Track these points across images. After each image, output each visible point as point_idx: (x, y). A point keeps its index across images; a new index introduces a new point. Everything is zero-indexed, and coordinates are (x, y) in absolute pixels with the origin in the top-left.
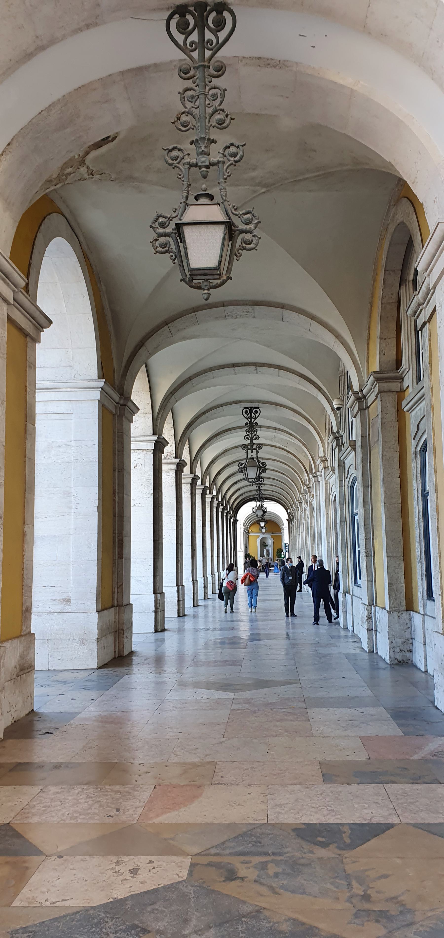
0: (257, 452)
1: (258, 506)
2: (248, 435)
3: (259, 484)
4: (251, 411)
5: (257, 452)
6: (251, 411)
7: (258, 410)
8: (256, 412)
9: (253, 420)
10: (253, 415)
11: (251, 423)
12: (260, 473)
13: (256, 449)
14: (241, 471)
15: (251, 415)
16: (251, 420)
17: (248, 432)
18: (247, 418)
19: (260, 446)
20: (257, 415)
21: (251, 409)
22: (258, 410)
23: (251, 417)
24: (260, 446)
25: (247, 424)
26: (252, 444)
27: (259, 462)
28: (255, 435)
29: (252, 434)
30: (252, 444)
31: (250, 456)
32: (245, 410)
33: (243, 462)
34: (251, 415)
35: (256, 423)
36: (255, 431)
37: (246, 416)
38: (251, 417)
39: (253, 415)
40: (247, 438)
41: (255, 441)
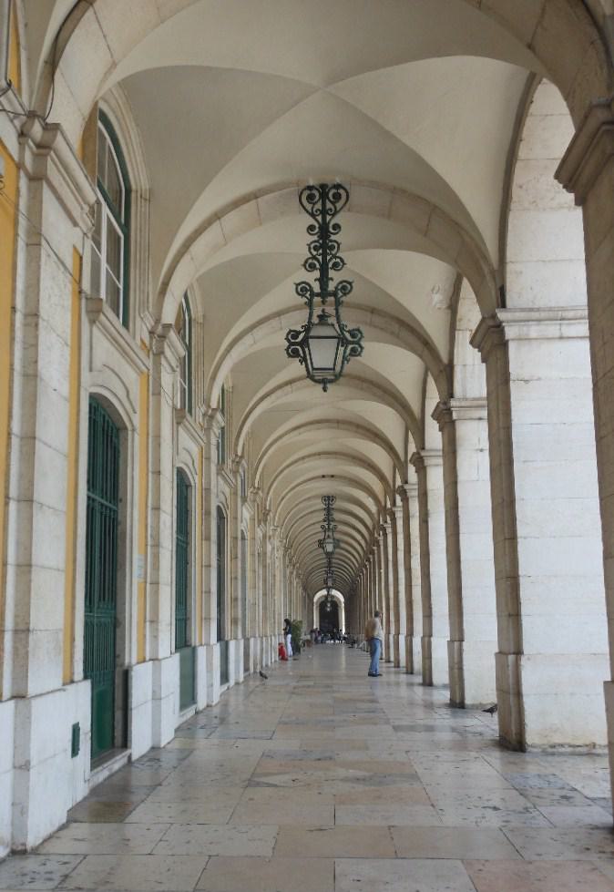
0: (338, 303)
2: (314, 257)
4: (324, 196)
5: (338, 303)
6: (324, 196)
7: (341, 191)
8: (337, 197)
9: (328, 218)
10: (329, 205)
12: (345, 359)
13: (334, 294)
14: (294, 354)
15: (324, 204)
17: (315, 248)
18: (313, 215)
19: (345, 287)
20: (339, 205)
21: (323, 189)
22: (341, 191)
24: (345, 287)
25: (311, 228)
26: (324, 280)
27: (342, 328)
28: (336, 257)
29: (324, 255)
30: (324, 280)
31: (317, 311)
33: (299, 328)
34: (324, 204)
35: (337, 227)
36: (332, 248)
37: (309, 207)
38: (324, 212)
39: (329, 205)
40: (312, 267)
41: (332, 273)
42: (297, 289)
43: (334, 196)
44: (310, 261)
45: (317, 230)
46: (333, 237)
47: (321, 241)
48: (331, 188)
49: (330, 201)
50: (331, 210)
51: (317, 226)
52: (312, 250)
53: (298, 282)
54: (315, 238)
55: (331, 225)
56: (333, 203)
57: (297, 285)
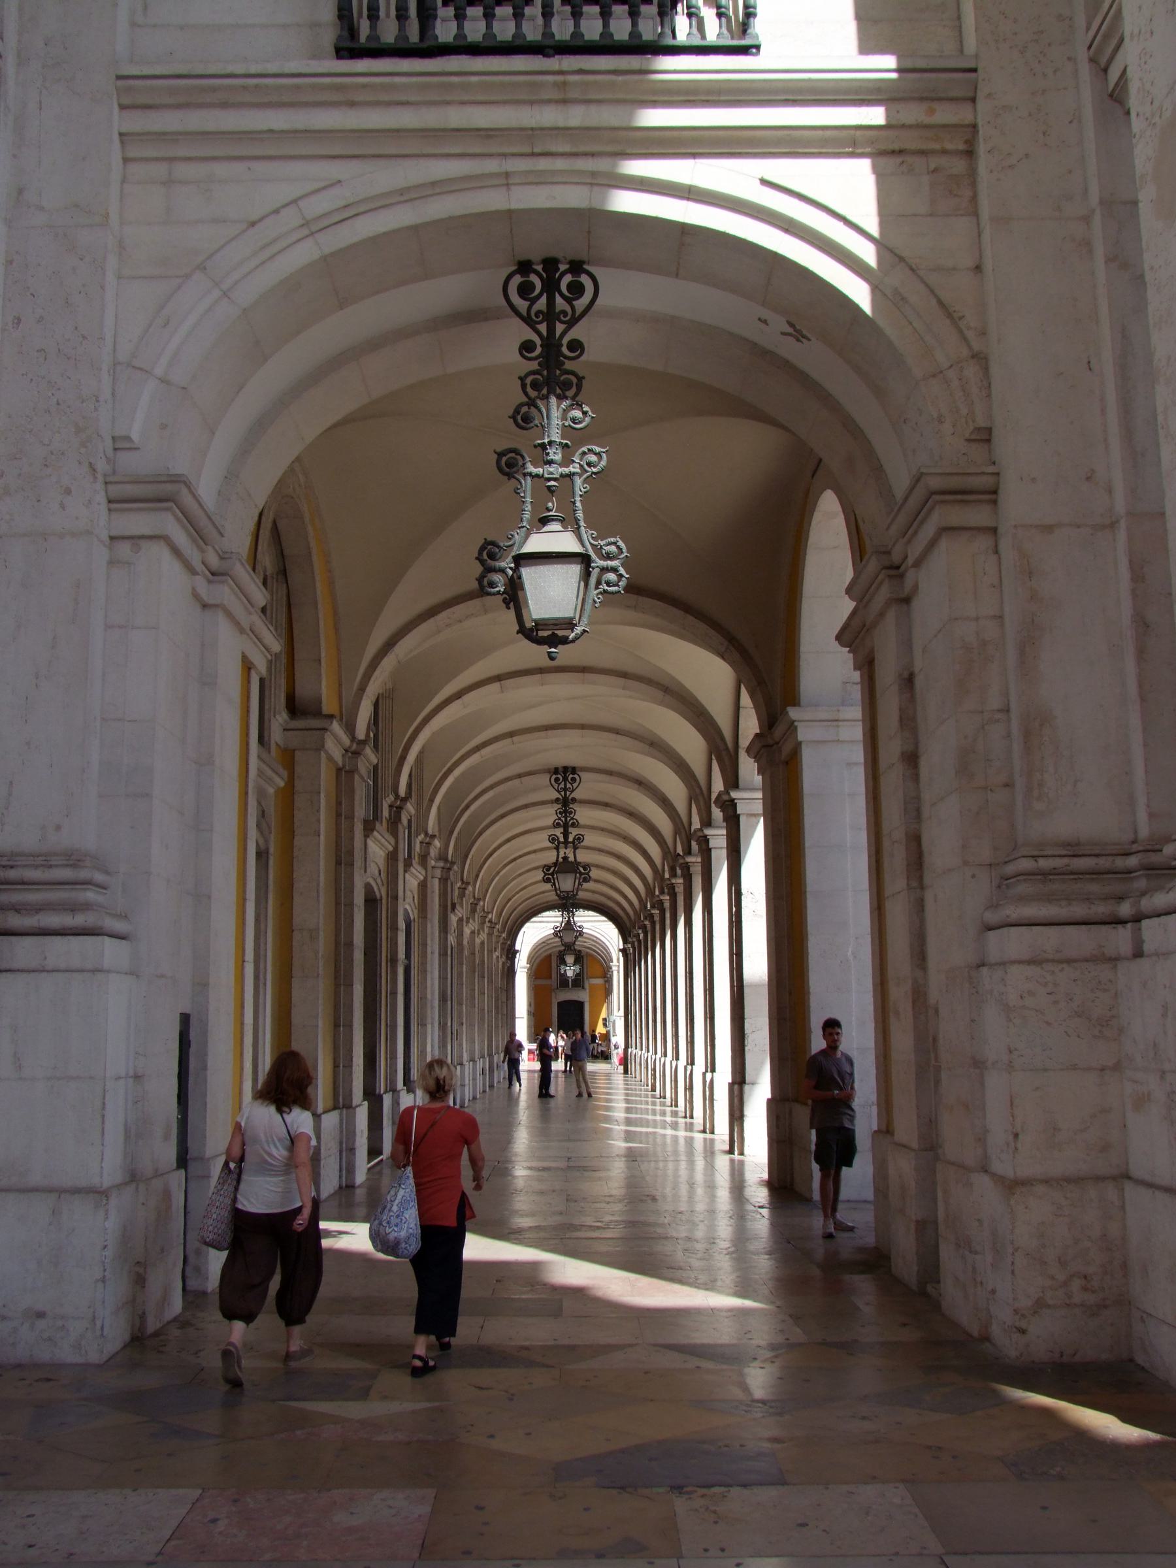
1: (560, 860)
3: (565, 789)
4: (551, 286)
6: (551, 286)
7: (584, 279)
8: (577, 289)
9: (560, 328)
11: (551, 345)
15: (551, 303)
16: (551, 329)
17: (535, 386)
18: (528, 320)
23: (551, 315)
25: (526, 347)
32: (517, 280)
34: (551, 303)
35: (576, 346)
37: (522, 304)
38: (551, 315)
42: (498, 462)
43: (569, 286)
44: (524, 409)
45: (539, 350)
46: (569, 365)
47: (545, 373)
48: (563, 274)
49: (562, 295)
50: (565, 313)
51: (538, 341)
52: (529, 389)
53: (499, 450)
54: (534, 366)
55: (565, 341)
56: (569, 301)
57: (500, 455)
